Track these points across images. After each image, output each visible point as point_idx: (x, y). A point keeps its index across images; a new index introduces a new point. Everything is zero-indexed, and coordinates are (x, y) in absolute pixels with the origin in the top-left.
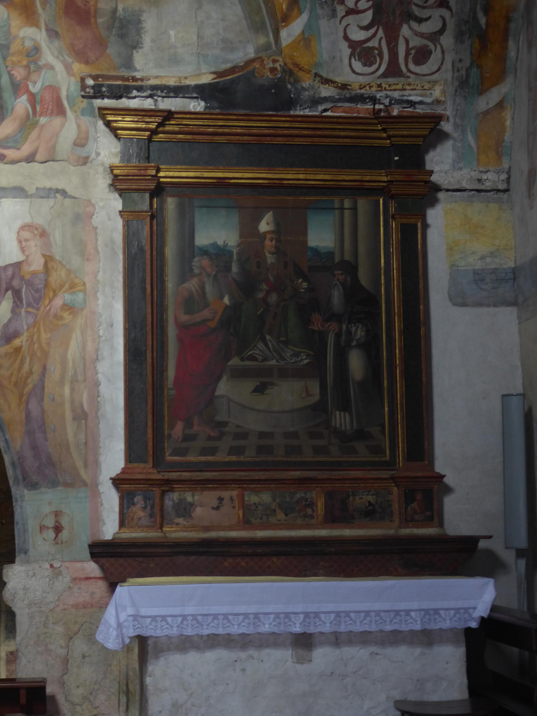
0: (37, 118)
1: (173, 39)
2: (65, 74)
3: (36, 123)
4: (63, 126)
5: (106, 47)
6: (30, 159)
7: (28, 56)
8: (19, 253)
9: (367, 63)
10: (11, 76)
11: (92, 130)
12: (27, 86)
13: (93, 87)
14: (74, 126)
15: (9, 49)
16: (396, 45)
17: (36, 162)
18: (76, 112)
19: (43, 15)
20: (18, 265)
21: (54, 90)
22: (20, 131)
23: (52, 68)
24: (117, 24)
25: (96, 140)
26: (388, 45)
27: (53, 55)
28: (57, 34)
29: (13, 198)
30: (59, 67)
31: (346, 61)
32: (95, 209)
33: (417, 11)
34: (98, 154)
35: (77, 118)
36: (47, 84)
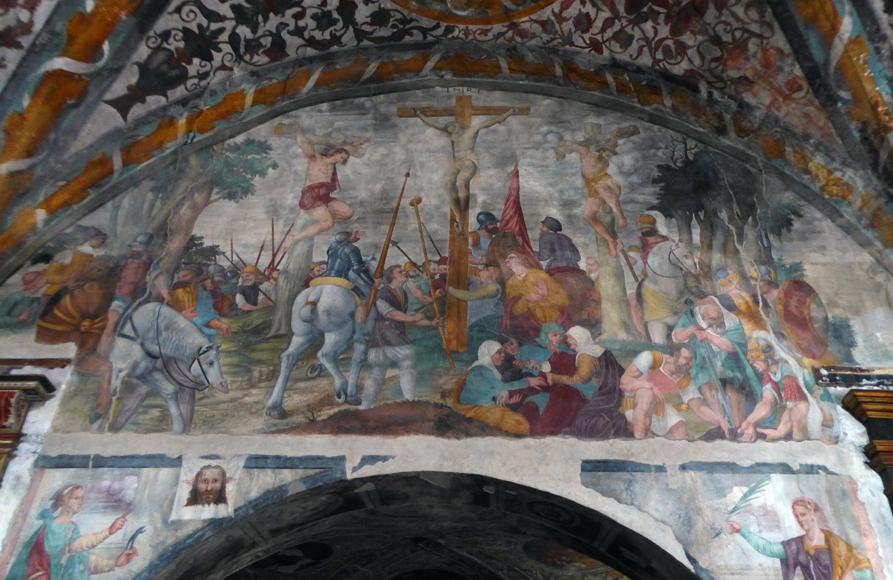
0: (784, 403)
1: (881, 340)
2: (798, 366)
3: (784, 408)
4: (808, 409)
5: (827, 346)
6: (788, 437)
7: (764, 352)
8: (799, 527)
10: (754, 368)
11: (833, 413)
12: (769, 376)
13: (828, 376)
14: (818, 410)
15: (747, 347)
17: (794, 440)
18: (816, 398)
19: (769, 323)
20: (800, 540)
21: (792, 378)
22: (773, 414)
23: (786, 362)
24: (831, 329)
25: (839, 422)
27: (783, 351)
28: (783, 335)
29: (781, 473)
30: (792, 361)
32: (857, 485)
34: (846, 434)
35: (817, 402)
36: (785, 374)
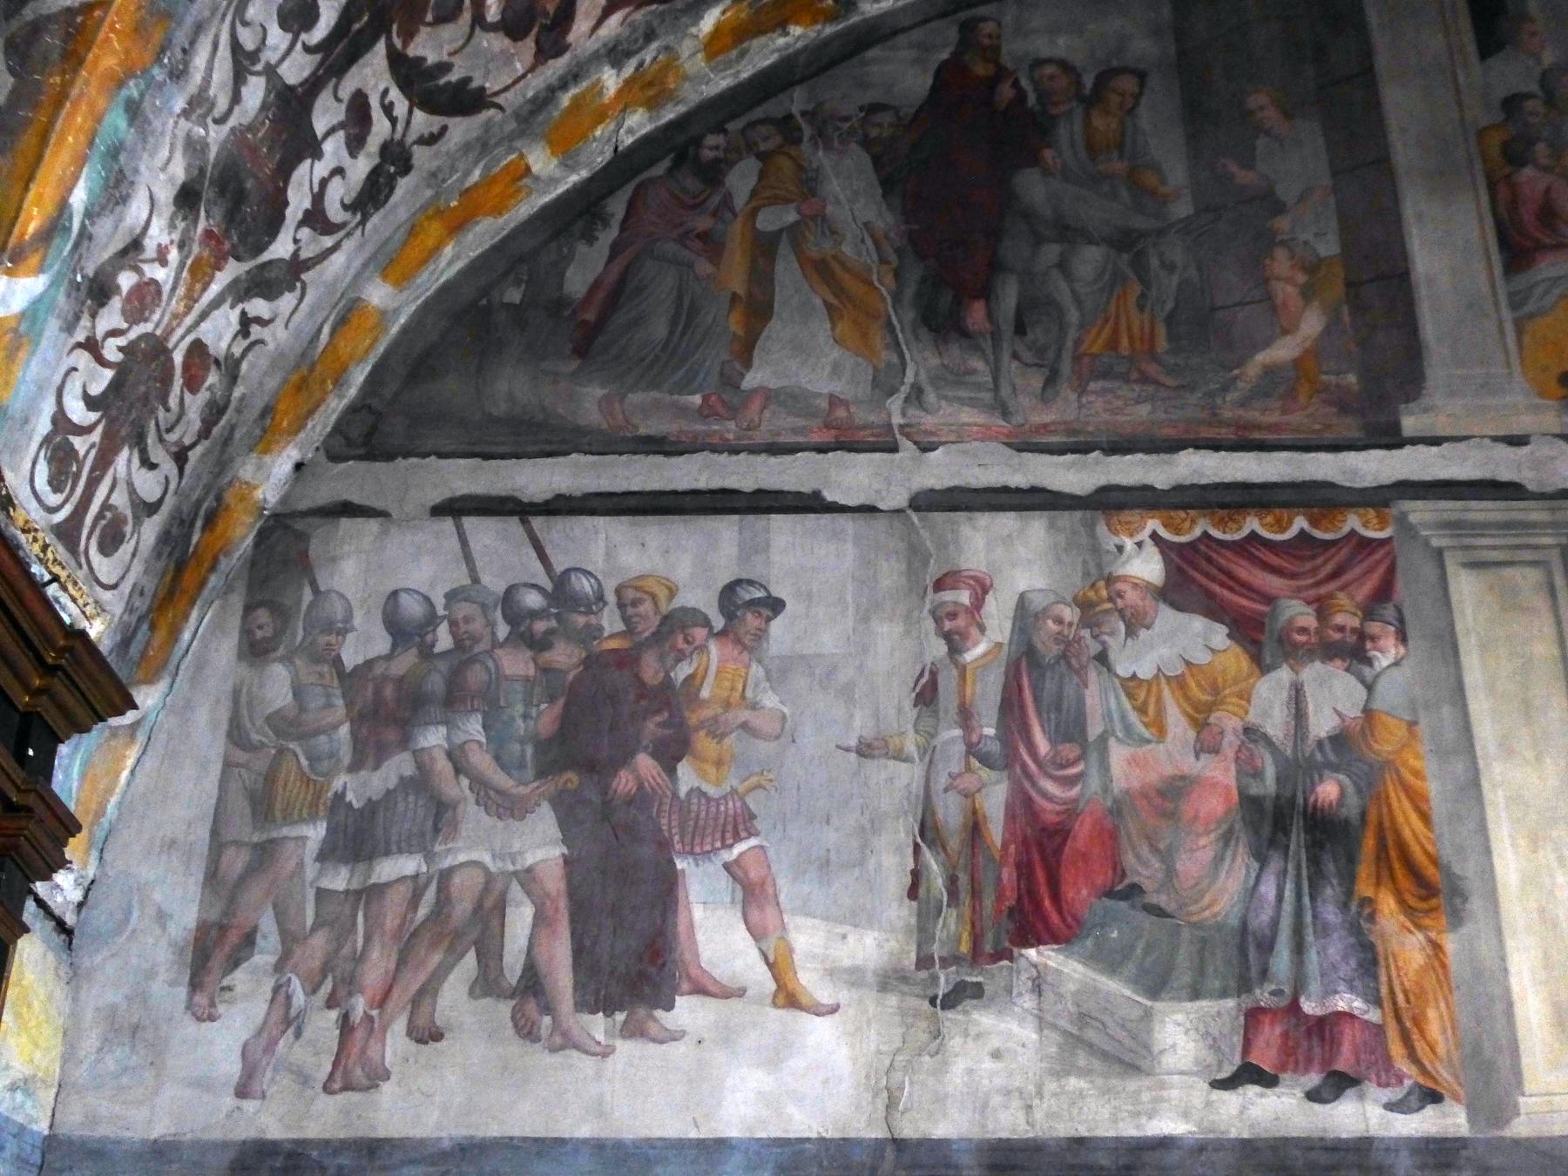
9: (56, 484)
16: (101, 477)
26: (92, 470)
31: (34, 446)
33: (151, 440)
